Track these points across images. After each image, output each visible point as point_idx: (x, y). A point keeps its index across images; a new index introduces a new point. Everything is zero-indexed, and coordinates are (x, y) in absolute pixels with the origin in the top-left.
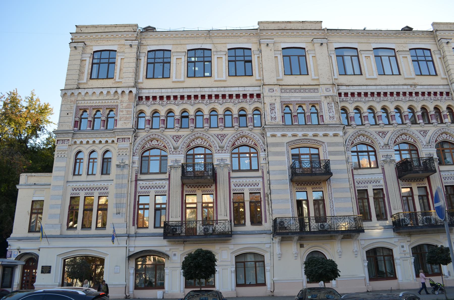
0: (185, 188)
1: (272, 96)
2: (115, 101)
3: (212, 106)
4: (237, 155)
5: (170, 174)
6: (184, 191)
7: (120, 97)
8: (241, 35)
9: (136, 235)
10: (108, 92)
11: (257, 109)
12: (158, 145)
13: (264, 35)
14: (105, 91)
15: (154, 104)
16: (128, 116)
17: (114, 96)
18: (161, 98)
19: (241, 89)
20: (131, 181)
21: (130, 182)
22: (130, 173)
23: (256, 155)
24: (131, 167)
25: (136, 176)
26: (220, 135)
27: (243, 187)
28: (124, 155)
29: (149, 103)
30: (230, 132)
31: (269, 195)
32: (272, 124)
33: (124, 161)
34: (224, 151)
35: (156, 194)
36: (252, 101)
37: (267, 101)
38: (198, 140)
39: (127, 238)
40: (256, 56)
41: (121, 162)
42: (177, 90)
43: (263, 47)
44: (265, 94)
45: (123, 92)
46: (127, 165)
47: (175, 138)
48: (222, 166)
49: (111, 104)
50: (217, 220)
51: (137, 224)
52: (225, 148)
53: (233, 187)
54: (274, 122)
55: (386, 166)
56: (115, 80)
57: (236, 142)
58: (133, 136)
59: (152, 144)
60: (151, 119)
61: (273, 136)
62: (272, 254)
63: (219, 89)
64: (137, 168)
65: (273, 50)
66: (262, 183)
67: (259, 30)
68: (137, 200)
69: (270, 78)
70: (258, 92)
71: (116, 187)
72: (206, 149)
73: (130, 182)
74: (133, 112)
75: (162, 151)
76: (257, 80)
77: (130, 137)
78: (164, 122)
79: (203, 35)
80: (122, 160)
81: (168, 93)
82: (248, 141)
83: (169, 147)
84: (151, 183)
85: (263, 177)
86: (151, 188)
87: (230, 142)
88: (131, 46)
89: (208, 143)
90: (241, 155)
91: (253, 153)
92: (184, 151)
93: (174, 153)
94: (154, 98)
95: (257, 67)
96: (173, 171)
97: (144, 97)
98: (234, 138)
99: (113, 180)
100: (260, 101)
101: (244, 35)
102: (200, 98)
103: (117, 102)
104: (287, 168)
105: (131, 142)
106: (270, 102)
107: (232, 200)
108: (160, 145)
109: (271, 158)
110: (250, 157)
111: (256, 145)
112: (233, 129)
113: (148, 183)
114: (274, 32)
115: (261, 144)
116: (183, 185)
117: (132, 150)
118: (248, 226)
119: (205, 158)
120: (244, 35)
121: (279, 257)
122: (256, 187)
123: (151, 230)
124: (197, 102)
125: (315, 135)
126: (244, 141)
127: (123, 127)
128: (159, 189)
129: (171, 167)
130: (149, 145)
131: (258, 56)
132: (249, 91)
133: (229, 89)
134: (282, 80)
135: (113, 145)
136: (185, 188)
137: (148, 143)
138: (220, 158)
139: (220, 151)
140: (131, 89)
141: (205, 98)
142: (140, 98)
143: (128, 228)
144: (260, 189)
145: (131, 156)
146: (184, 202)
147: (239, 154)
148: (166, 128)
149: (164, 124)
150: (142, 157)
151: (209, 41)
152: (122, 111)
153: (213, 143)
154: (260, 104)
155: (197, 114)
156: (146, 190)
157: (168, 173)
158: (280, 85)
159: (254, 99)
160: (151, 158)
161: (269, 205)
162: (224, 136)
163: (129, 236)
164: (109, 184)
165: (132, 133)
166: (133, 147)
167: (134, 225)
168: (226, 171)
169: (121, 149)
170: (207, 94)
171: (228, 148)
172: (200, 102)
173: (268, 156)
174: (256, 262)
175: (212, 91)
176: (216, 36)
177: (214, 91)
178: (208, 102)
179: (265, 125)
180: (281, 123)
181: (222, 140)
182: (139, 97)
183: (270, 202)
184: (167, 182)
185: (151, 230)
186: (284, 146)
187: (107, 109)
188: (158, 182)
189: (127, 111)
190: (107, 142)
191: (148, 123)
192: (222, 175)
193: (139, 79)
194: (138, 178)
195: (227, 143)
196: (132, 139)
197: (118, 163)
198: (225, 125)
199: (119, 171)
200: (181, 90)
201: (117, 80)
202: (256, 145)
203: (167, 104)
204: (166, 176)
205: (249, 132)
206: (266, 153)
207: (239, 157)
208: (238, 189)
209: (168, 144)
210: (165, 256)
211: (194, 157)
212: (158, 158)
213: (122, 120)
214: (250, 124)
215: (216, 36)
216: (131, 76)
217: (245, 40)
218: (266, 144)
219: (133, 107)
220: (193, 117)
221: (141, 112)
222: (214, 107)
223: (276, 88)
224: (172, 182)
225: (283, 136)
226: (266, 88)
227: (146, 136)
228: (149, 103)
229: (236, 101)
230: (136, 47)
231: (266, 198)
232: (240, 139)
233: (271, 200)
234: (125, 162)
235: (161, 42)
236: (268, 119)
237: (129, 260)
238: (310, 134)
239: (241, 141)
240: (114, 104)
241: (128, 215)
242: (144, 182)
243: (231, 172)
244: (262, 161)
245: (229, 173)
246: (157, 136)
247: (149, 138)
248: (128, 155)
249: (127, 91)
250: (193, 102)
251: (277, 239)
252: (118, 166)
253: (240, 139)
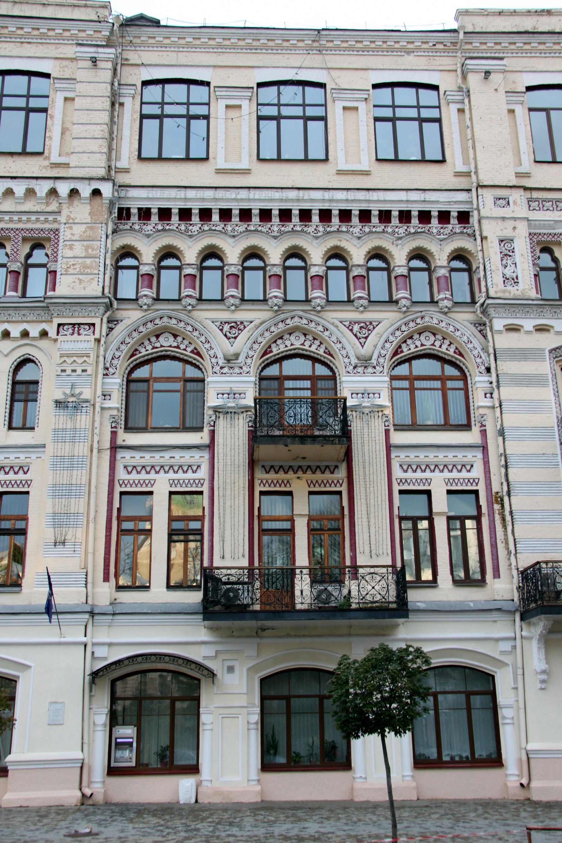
0: (260, 475)
1: (503, 219)
2: (51, 218)
3: (332, 242)
4: (406, 384)
5: (212, 433)
6: (257, 482)
7: (64, 206)
8: (410, 46)
9: (115, 612)
10: (30, 192)
11: (460, 255)
12: (178, 347)
13: (476, 49)
14: (19, 188)
15: (164, 230)
16: (88, 261)
17: (48, 204)
18: (185, 214)
19: (414, 196)
20: (99, 451)
21: (95, 451)
22: (97, 424)
23: (460, 384)
24: (98, 409)
25: (114, 434)
26: (359, 323)
27: (428, 474)
28: (79, 372)
29: (150, 227)
30: (387, 320)
31: (506, 499)
32: (507, 295)
33: (77, 391)
34: (370, 370)
35: (174, 489)
36: (447, 231)
37: (492, 231)
38: (292, 338)
39: (87, 616)
40: (454, 108)
41: (68, 391)
42: (231, 194)
43: (474, 80)
44: (483, 213)
45: (74, 193)
46: (87, 401)
47: (226, 328)
48: (366, 411)
49: (38, 226)
50: (355, 568)
51: (116, 576)
52: (374, 361)
53: (398, 473)
54: (513, 291)
56: (48, 158)
57: (404, 346)
58: (105, 320)
59: (158, 345)
60: (155, 273)
61: (513, 329)
62: (520, 672)
63: (351, 195)
64: (115, 412)
65: (502, 91)
66: (481, 462)
67: (461, 35)
68: (116, 505)
69: (496, 168)
70: (463, 208)
71: (54, 466)
72: (317, 365)
73: (95, 451)
74: (103, 251)
75: (188, 367)
76: (458, 174)
77: (97, 321)
78: (194, 282)
79: (300, 44)
80: (73, 386)
81: (203, 200)
82: (438, 344)
83: (212, 353)
84: (157, 455)
85: (484, 448)
86: (157, 472)
87: (388, 345)
88: (94, 61)
89: (323, 347)
90: (417, 384)
91: (452, 378)
92: (254, 364)
93: (225, 370)
94: (165, 214)
95: (456, 136)
96: (222, 425)
97: (134, 211)
98: (398, 333)
99: (44, 446)
100: (469, 231)
101: (418, 49)
102: (295, 219)
103: (55, 221)
104: (555, 420)
105: (97, 335)
106: (500, 234)
107: (396, 512)
108: (182, 347)
109: (507, 392)
110: (444, 390)
111: (461, 354)
112: (394, 308)
113: (147, 456)
114: (505, 40)
115: (475, 352)
116: (252, 463)
117: (101, 359)
118: (446, 591)
119: (313, 389)
120: (418, 49)
121: (543, 681)
122: (464, 474)
123: (159, 594)
124: (287, 229)
126: (428, 344)
127: (75, 293)
128: (180, 475)
129: (216, 410)
130: (149, 347)
131: (460, 106)
132: (438, 202)
133: (381, 195)
134: (527, 175)
135: (44, 343)
136: (260, 475)
137: (146, 343)
138: (365, 388)
139: (360, 370)
140: (96, 185)
141: (310, 220)
142: (124, 214)
143: (89, 585)
144: (475, 481)
145: (100, 376)
146: (256, 513)
147: (412, 379)
148: (200, 300)
149: (194, 288)
150: (129, 381)
151: (315, 60)
152: (71, 248)
153: (339, 346)
154: (472, 240)
155: (288, 263)
156: (143, 476)
157: (206, 430)
158: (526, 189)
159: (450, 226)
160: (157, 386)
161: (505, 526)
162: (368, 326)
163: (92, 614)
164: (33, 456)
165: (102, 309)
166: (106, 351)
167: (106, 578)
168: (377, 427)
169: (69, 356)
170: (315, 208)
171: (381, 360)
172: (298, 228)
173: (498, 387)
174: (468, 695)
175: (331, 201)
176: (338, 48)
177: (338, 201)
178: (321, 229)
179: (488, 297)
180: (533, 294)
181: (362, 339)
182: (120, 210)
183: (508, 518)
184: (206, 455)
185: (159, 594)
186: (544, 360)
187: (25, 239)
188: (177, 454)
189: (87, 248)
190: (25, 334)
191: (146, 283)
192: (368, 438)
193: (118, 159)
194: (119, 442)
195: (379, 346)
196: (101, 328)
197: (59, 396)
198: (369, 295)
199: (63, 420)
200: (243, 194)
201: (55, 158)
202: (461, 354)
203: (201, 231)
204: (201, 438)
205: (442, 317)
206: (494, 378)
207: (412, 390)
208: (415, 479)
209: (207, 346)
210: (205, 672)
211: (281, 386)
212: (178, 386)
213: (71, 271)
214: (442, 296)
215: (338, 48)
216: (95, 148)
217: (422, 62)
218: (491, 351)
219: (104, 237)
220: (278, 271)
221: (128, 252)
222: (339, 244)
223: (516, 196)
224: (221, 457)
225: (541, 329)
226: (488, 196)
227: (144, 321)
228: (149, 228)
229: (401, 231)
230: (109, 65)
231: (497, 507)
232: (416, 336)
233: (511, 512)
234: (80, 394)
235: (183, 58)
236: (495, 284)
237: (93, 682)
239: (418, 343)
240: (47, 226)
241: (90, 550)
242: (137, 455)
243: (392, 428)
244: (479, 400)
245: (387, 432)
246: (174, 321)
247: (150, 325)
248: (89, 372)
249: (85, 190)
250: (276, 229)
251: (540, 625)
252: (59, 404)
253: (416, 336)
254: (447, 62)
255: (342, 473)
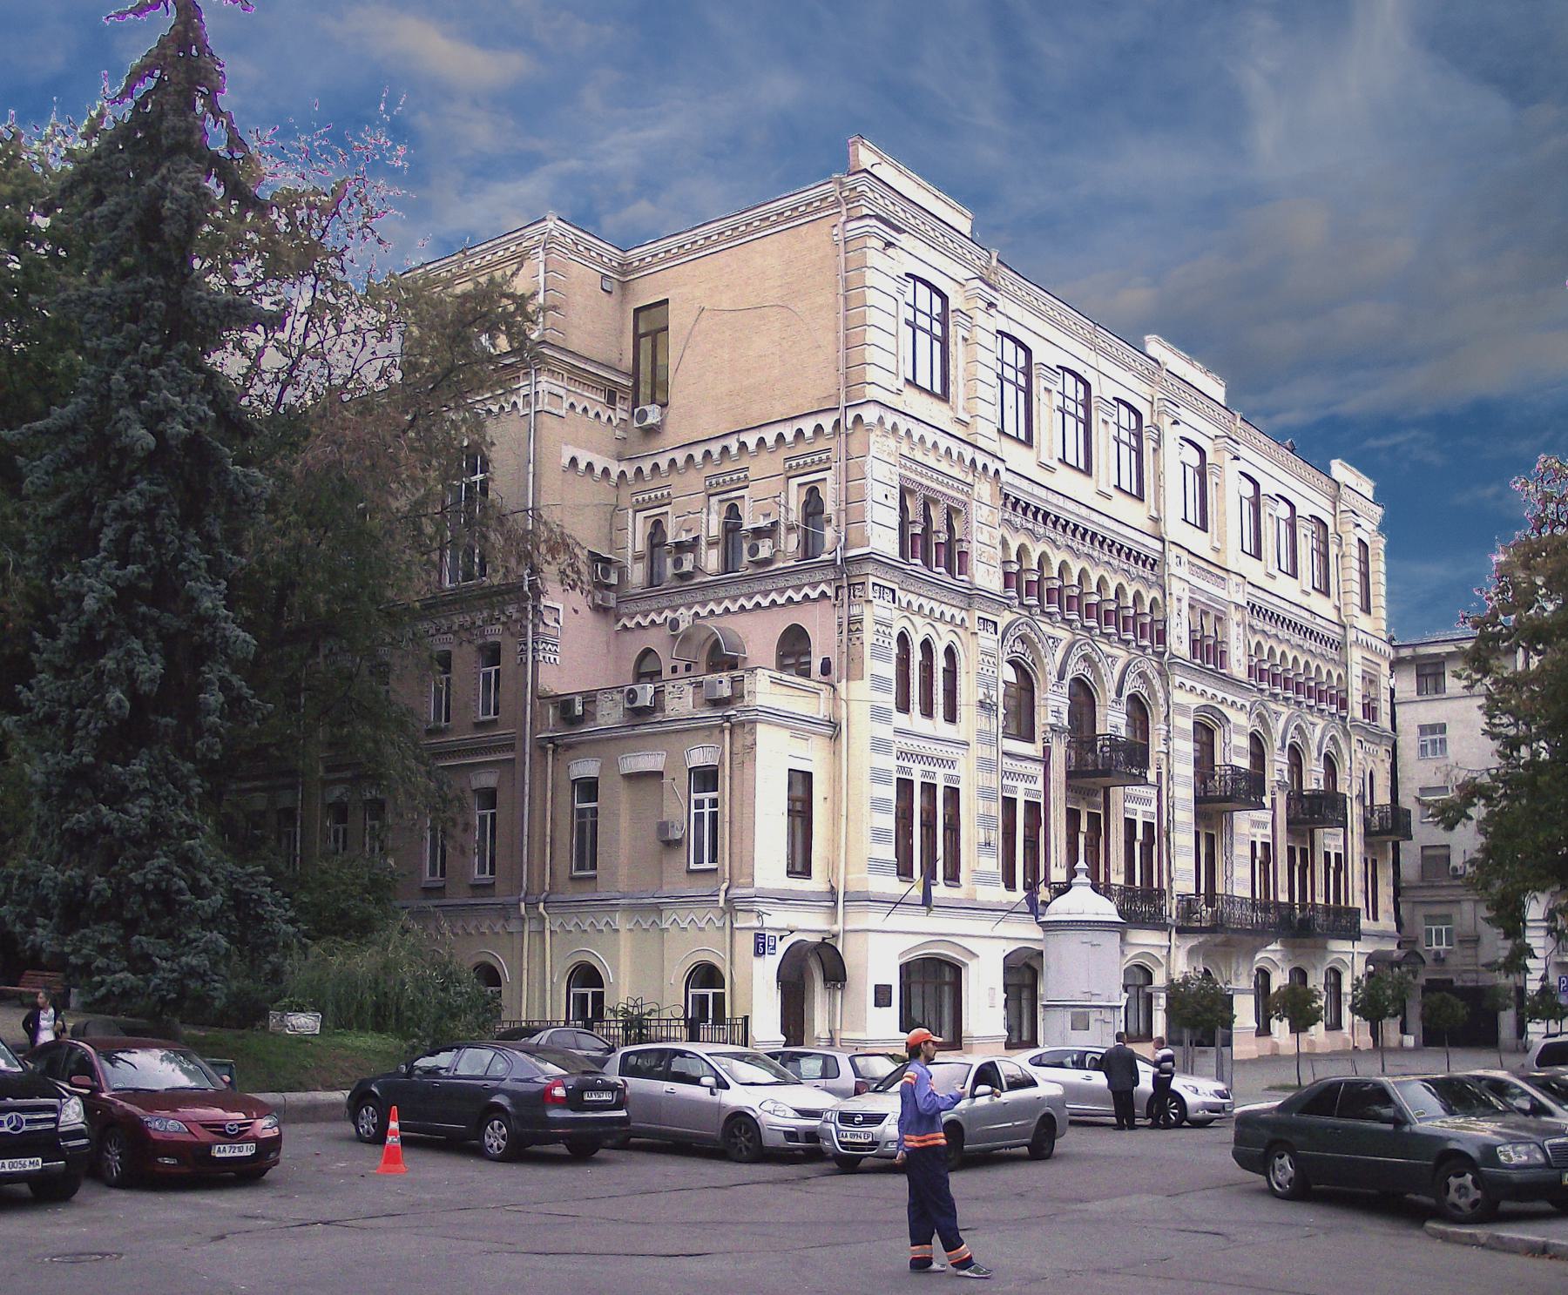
5: (1047, 751)
55: (1278, 796)
61: (1182, 685)
70: (1156, 556)
76: (1152, 518)
125: (1224, 700)
129: (1053, 728)
223: (1185, 556)
238: (1220, 695)
254: (1144, 389)
255: (1100, 799)
